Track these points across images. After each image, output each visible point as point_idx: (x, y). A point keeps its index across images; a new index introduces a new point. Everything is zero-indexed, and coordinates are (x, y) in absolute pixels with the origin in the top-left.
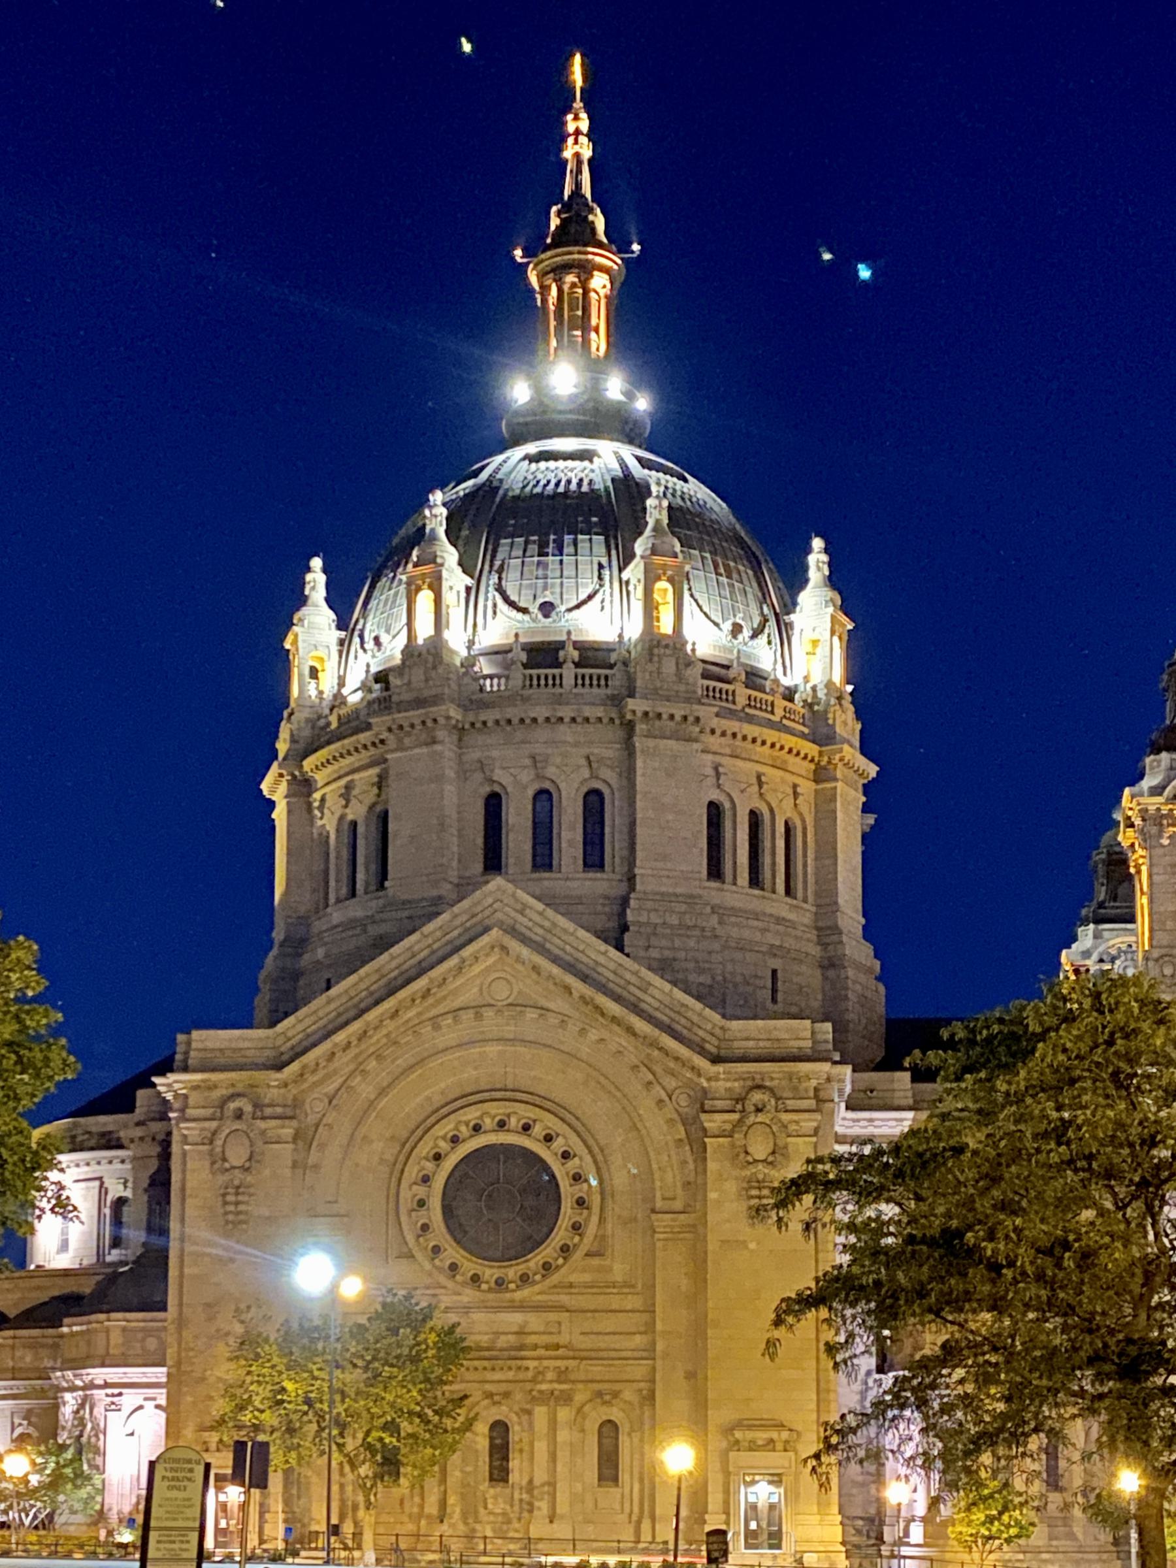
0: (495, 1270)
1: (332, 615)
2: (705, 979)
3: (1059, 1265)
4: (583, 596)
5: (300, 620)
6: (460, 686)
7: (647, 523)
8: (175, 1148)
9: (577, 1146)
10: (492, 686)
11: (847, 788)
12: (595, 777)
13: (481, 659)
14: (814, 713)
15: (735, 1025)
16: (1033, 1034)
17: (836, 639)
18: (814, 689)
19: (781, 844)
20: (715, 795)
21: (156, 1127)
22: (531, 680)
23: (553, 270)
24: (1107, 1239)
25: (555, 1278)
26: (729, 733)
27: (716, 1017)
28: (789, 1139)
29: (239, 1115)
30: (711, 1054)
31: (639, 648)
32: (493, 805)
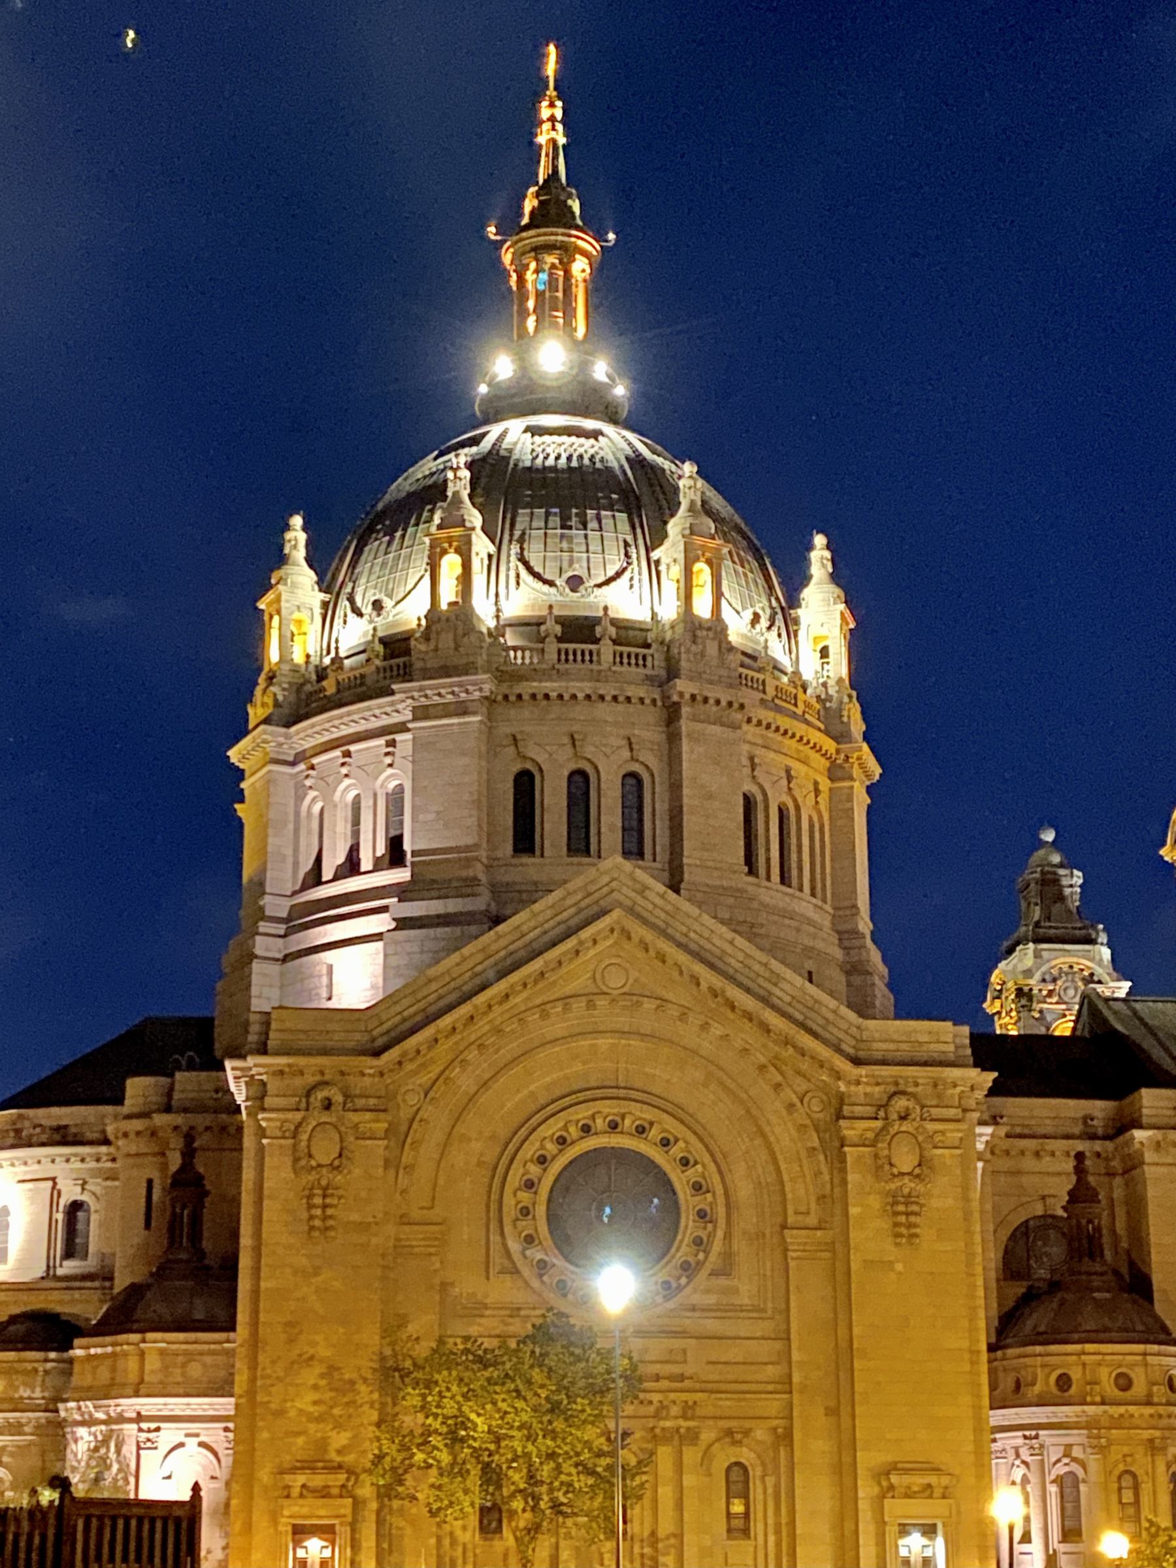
1: (311, 576)
4: (611, 573)
9: (698, 1151)
13: (508, 631)
15: (871, 1024)
26: (764, 723)
29: (328, 1105)
31: (679, 629)
32: (525, 784)
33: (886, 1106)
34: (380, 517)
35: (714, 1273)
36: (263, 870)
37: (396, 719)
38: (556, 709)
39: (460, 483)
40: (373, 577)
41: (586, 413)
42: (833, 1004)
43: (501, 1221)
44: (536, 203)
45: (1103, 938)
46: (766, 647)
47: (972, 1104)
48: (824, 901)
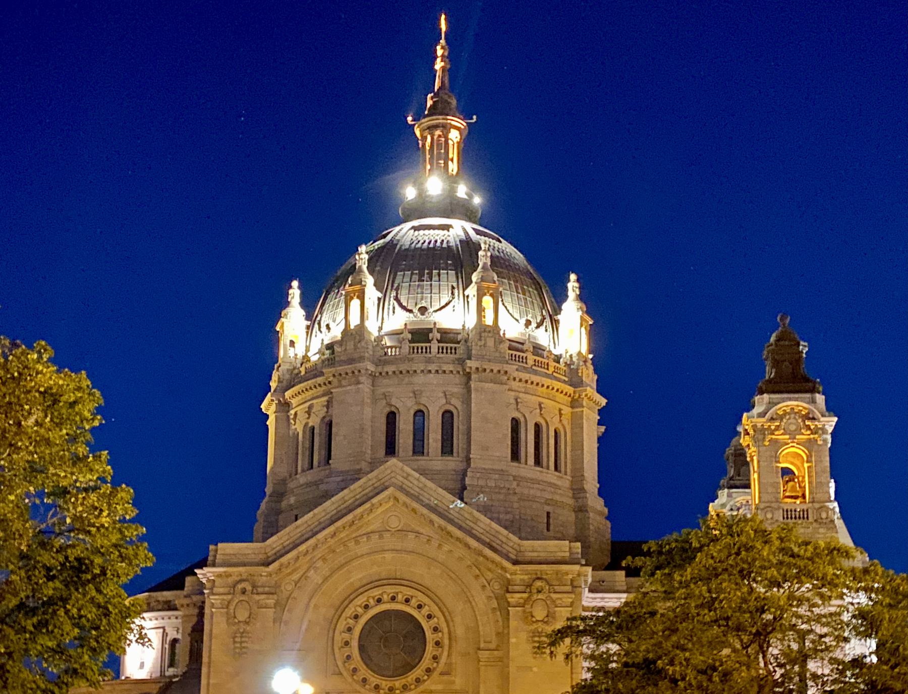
0: (388, 683)
1: (303, 312)
2: (508, 517)
3: (710, 679)
4: (443, 304)
5: (285, 315)
6: (374, 352)
7: (479, 265)
8: (207, 611)
10: (391, 352)
11: (589, 411)
12: (448, 403)
13: (386, 337)
14: (571, 370)
15: (525, 542)
16: (695, 548)
17: (583, 329)
18: (571, 356)
19: (552, 442)
20: (517, 415)
21: (196, 598)
22: (413, 349)
23: (429, 128)
24: (737, 665)
25: (422, 688)
26: (523, 380)
27: (515, 539)
28: (557, 609)
29: (244, 592)
30: (512, 559)
32: (391, 418)
35: (442, 674)
40: (329, 311)
43: (333, 650)
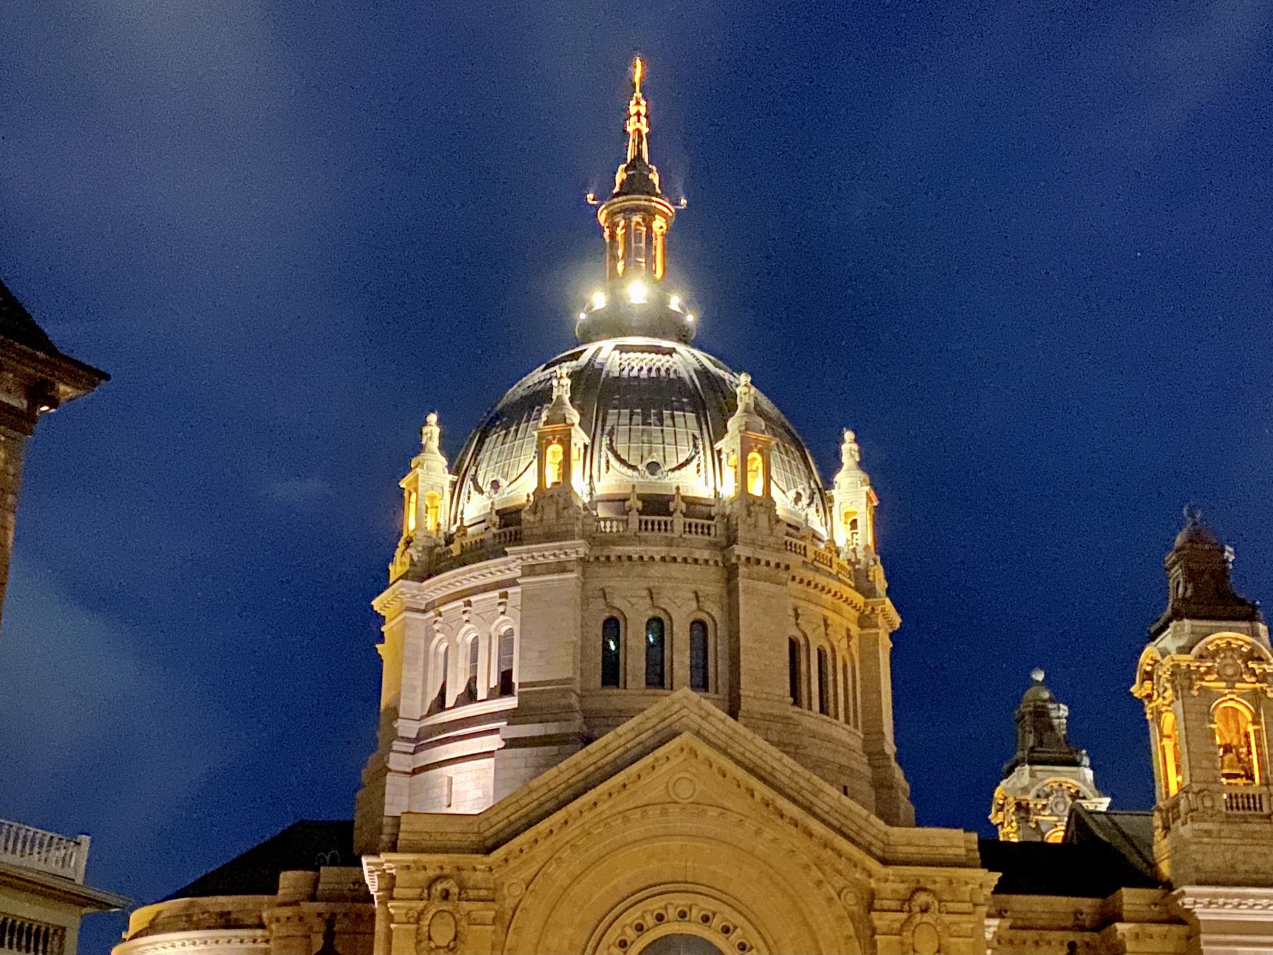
4: (682, 460)
12: (700, 609)
13: (600, 505)
14: (856, 570)
15: (895, 829)
18: (854, 550)
20: (794, 632)
29: (446, 895)
31: (737, 505)
32: (612, 627)
33: (910, 900)
34: (498, 416)
36: (398, 698)
37: (509, 575)
38: (639, 568)
39: (562, 389)
40: (492, 463)
41: (663, 335)
42: (865, 812)
44: (625, 176)
45: (1086, 761)
46: (806, 520)
47: (982, 900)
48: (856, 726)
